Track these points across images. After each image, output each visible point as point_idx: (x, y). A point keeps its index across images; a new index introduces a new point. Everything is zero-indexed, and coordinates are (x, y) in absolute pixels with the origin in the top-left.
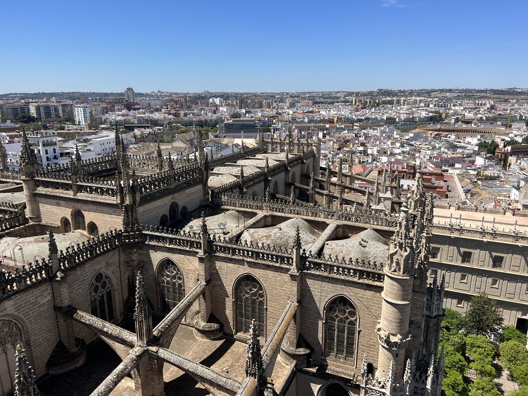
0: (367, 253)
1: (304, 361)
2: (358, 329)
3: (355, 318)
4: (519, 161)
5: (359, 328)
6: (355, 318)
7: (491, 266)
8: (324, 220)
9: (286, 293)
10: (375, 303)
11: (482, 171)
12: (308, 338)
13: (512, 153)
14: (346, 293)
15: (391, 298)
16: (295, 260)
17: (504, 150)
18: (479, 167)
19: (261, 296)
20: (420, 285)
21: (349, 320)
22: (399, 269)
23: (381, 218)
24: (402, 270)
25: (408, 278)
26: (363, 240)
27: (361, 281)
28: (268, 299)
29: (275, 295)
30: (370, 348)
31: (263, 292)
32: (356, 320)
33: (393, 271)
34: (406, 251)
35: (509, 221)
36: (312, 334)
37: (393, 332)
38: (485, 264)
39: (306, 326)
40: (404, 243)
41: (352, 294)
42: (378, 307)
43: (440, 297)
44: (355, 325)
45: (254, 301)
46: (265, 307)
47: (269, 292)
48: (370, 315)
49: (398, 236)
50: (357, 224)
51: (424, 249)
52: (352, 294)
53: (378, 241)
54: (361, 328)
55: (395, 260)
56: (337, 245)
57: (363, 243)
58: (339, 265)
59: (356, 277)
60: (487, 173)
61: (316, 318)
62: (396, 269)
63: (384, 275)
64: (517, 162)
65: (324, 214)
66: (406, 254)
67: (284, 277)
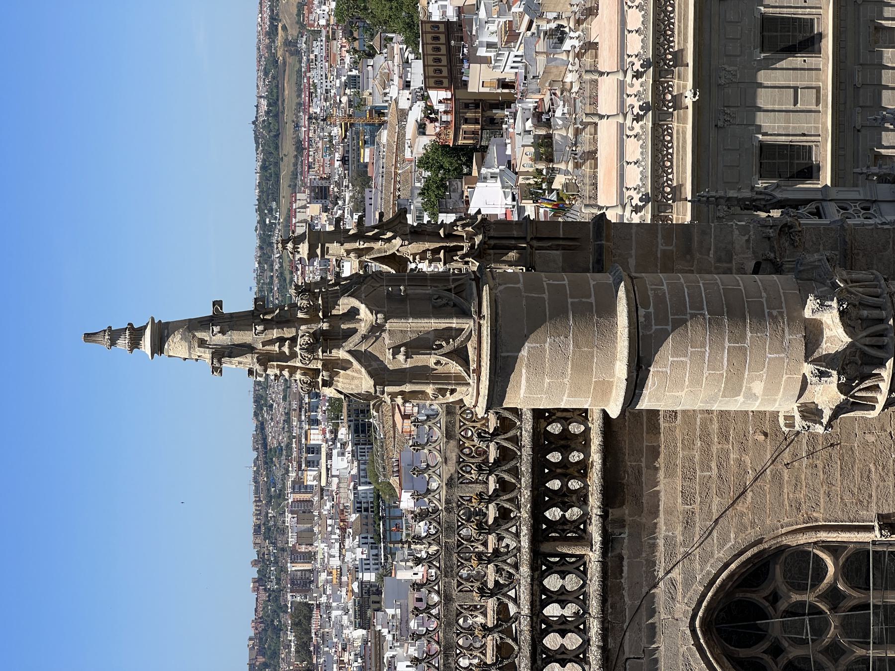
2: (876, 535)
4: (482, 52)
5: (870, 529)
7: (812, 61)
10: (706, 452)
11: (521, 181)
13: (456, 82)
15: (611, 361)
17: (446, 112)
18: (510, 198)
20: (564, 248)
22: (448, 334)
23: (448, 510)
24: (455, 323)
25: (486, 290)
27: (595, 531)
32: (834, 549)
33: (465, 362)
34: (353, 313)
35: (611, 22)
37: (796, 341)
38: (805, 84)
40: (314, 327)
42: (724, 436)
43: (806, 202)
44: (861, 554)
48: (777, 477)
49: (281, 357)
51: (378, 245)
54: (870, 516)
55: (401, 362)
60: (526, 160)
62: (447, 348)
64: (485, 60)
66: (364, 312)
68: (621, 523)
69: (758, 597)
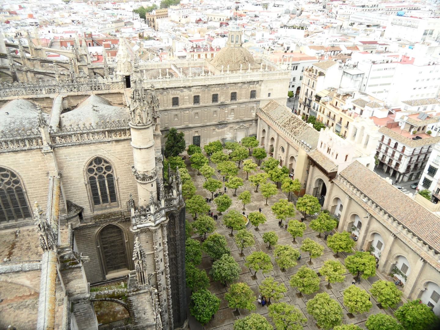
0: (102, 116)
1: (77, 220)
2: (116, 178)
3: (111, 171)
6: (111, 171)
8: (47, 96)
9: (43, 171)
10: (126, 154)
12: (76, 201)
14: (100, 154)
16: (44, 138)
19: (17, 182)
21: (106, 174)
26: (94, 106)
28: (25, 182)
29: (32, 177)
30: (129, 188)
31: (18, 178)
36: (78, 197)
39: (71, 193)
41: (105, 152)
45: (10, 190)
46: (24, 191)
47: (24, 176)
48: (123, 164)
50: (80, 93)
52: (105, 152)
53: (105, 104)
56: (72, 115)
57: (95, 108)
58: (88, 131)
59: (106, 137)
61: (78, 182)
63: (129, 129)
65: (45, 90)
67: (37, 157)
68: (112, 143)
69: (103, 163)
